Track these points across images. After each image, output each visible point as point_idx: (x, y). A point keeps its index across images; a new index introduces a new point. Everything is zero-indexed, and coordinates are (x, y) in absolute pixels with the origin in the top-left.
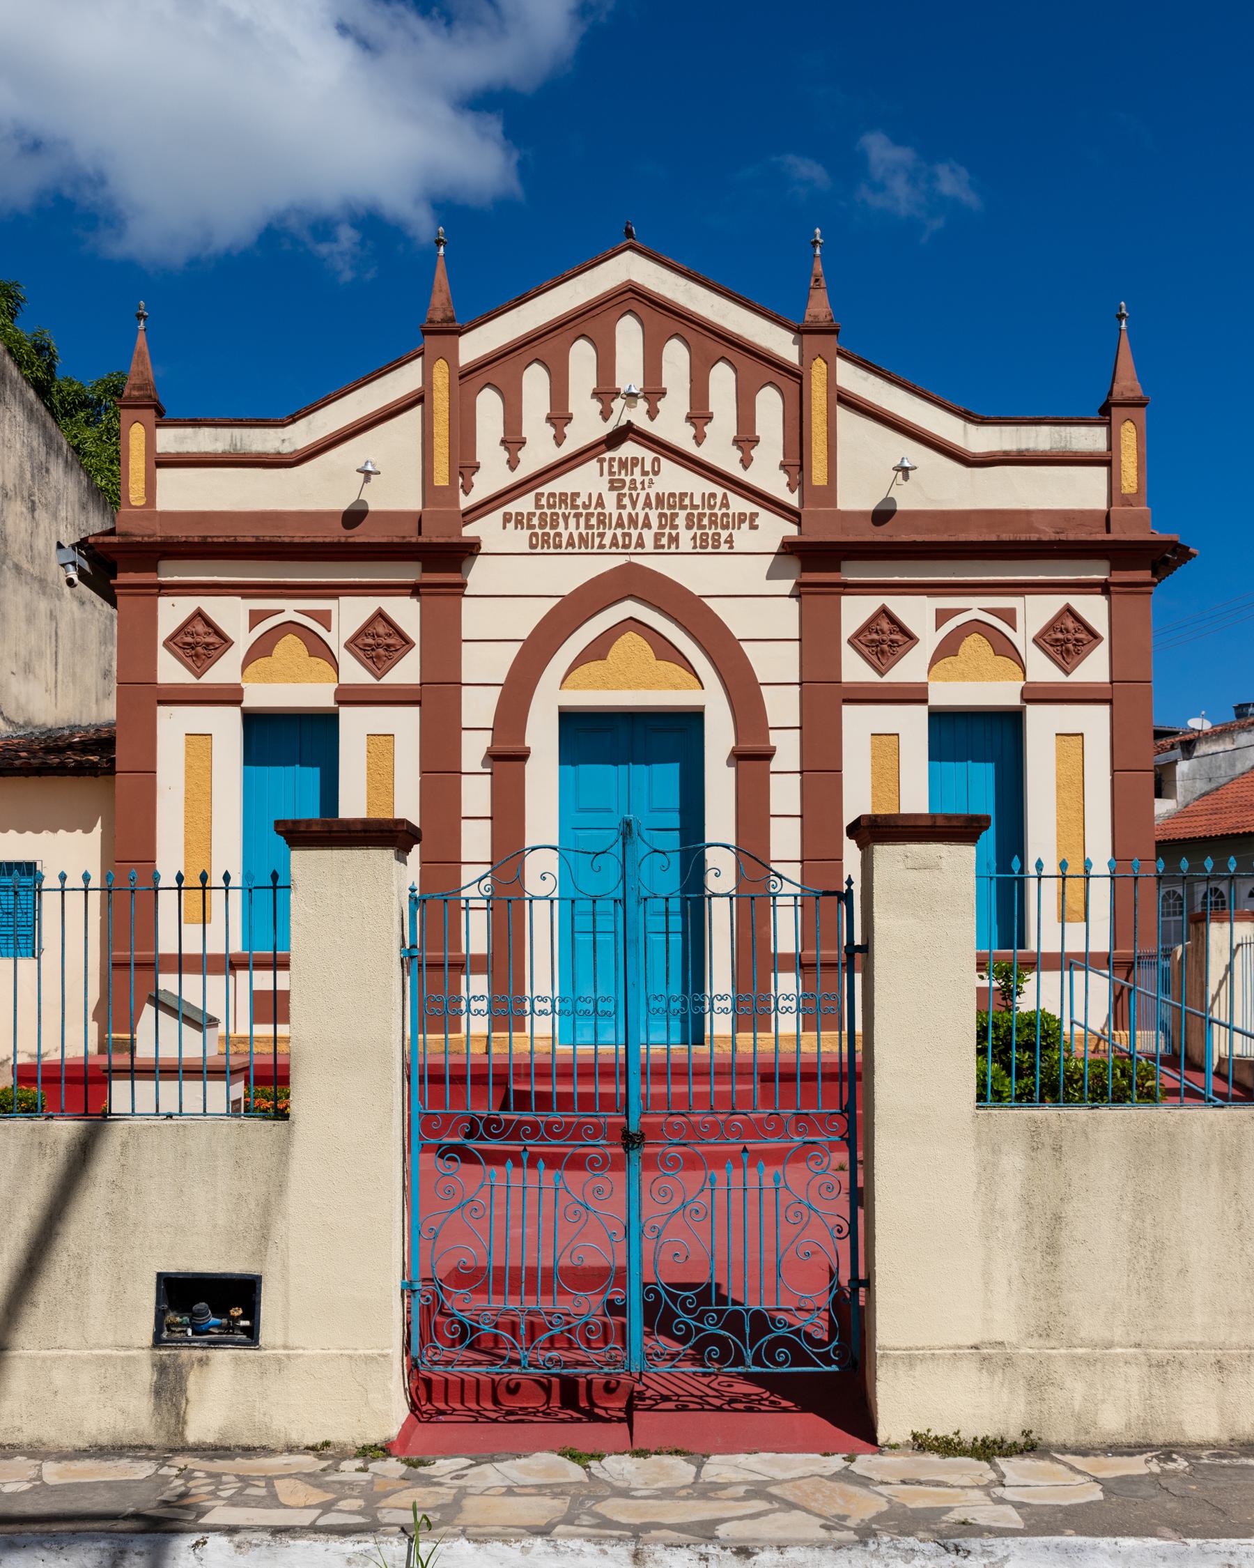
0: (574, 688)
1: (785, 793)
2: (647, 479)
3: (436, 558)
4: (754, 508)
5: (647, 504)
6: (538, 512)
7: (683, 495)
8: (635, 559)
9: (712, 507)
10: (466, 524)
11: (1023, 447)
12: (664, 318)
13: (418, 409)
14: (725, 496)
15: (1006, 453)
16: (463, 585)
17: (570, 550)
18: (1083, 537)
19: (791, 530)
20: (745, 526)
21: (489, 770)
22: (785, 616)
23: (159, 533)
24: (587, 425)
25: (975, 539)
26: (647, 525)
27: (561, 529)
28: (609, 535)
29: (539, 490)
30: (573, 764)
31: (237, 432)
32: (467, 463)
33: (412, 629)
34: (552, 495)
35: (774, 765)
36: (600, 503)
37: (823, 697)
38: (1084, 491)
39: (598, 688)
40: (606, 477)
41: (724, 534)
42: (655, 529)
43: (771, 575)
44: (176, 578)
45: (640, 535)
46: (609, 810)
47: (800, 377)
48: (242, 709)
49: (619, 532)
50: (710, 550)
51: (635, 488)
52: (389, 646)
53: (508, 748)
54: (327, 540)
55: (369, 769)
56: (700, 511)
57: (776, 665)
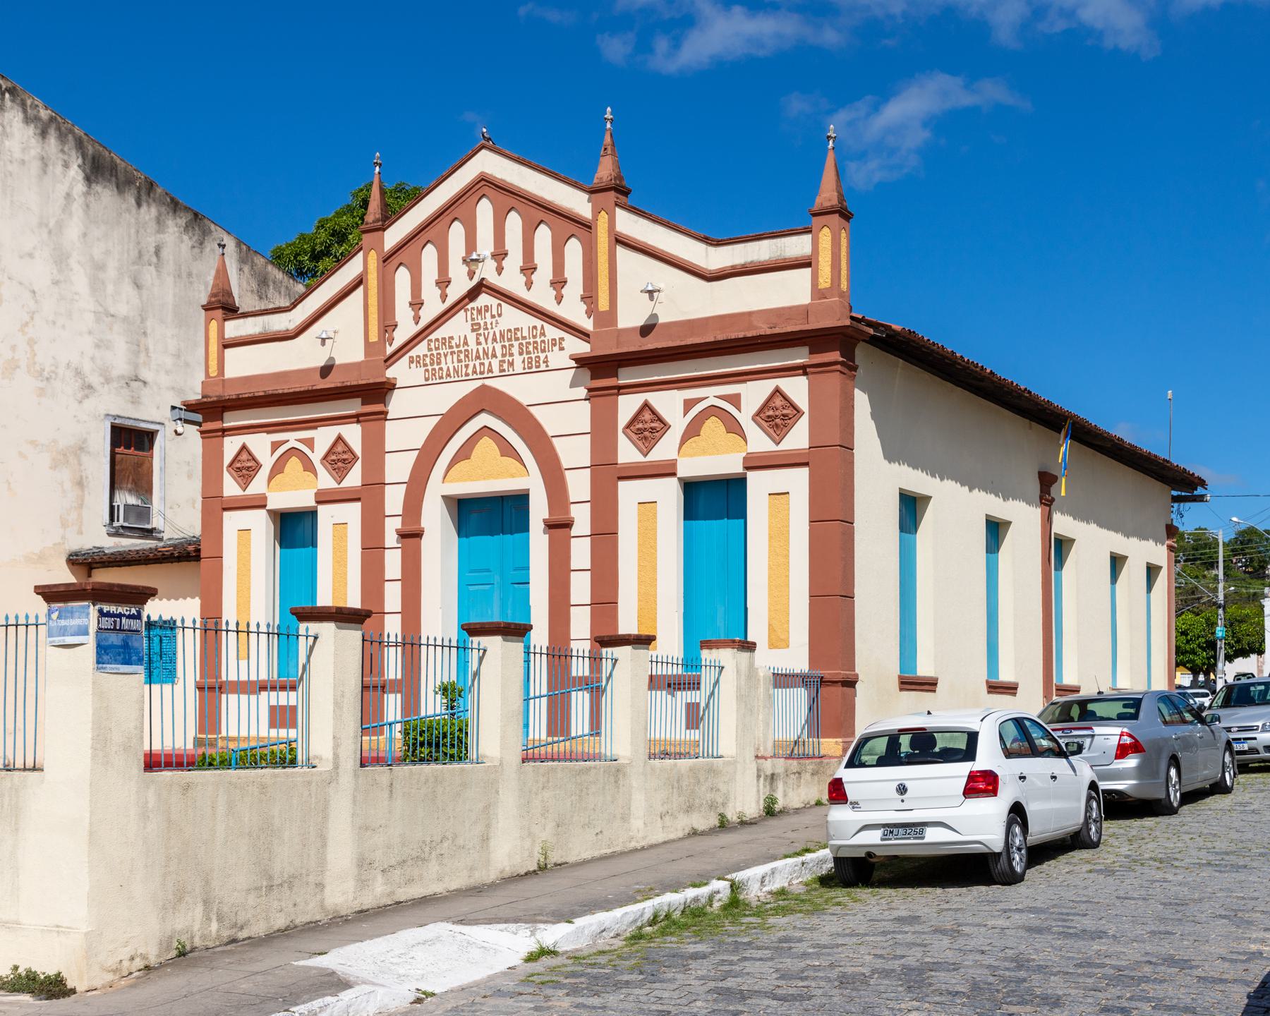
1: (581, 553)
5: (494, 340)
7: (517, 329)
8: (487, 382)
9: (534, 337)
10: (388, 367)
11: (749, 260)
13: (361, 288)
15: (733, 267)
16: (386, 413)
18: (789, 329)
19: (583, 348)
20: (556, 348)
22: (580, 415)
23: (231, 393)
24: (460, 285)
26: (494, 356)
27: (443, 365)
30: (467, 536)
31: (266, 318)
32: (388, 323)
33: (357, 448)
34: (437, 340)
36: (466, 343)
37: (608, 474)
40: (470, 322)
41: (542, 356)
42: (500, 358)
43: (573, 385)
44: (232, 424)
48: (272, 513)
49: (477, 363)
50: (534, 369)
53: (411, 528)
57: (575, 454)
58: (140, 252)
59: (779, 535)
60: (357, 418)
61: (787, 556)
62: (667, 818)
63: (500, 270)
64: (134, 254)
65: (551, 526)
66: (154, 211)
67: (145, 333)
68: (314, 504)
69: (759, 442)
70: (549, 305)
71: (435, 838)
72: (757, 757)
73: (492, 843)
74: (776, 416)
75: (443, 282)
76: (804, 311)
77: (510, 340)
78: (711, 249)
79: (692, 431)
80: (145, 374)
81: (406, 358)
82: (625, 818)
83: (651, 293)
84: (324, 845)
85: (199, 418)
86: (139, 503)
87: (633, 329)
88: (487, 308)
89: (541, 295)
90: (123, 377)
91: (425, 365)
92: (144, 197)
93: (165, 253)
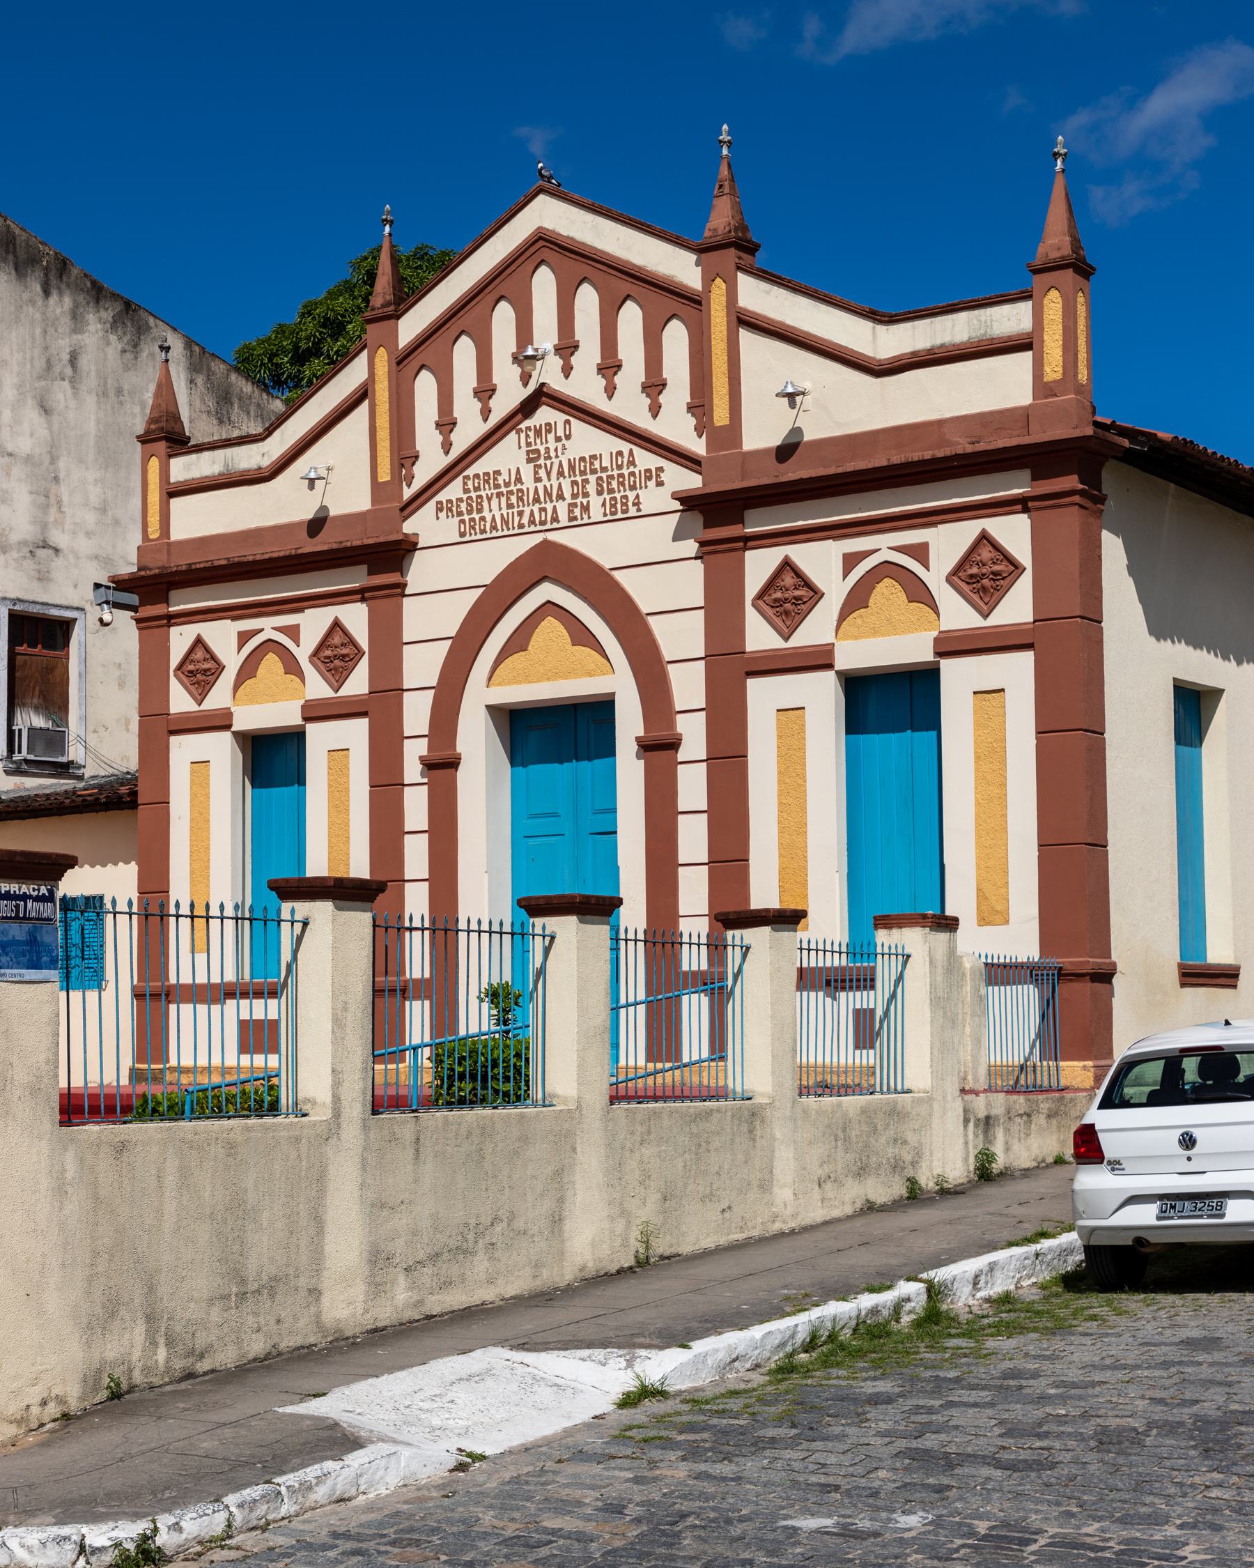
0: (499, 684)
1: (692, 786)
2: (559, 445)
3: (378, 559)
4: (661, 462)
5: (561, 474)
6: (465, 497)
7: (593, 457)
8: (551, 536)
9: (620, 467)
10: (406, 518)
11: (938, 342)
12: (577, 262)
13: (365, 405)
14: (631, 451)
15: (914, 354)
16: (405, 585)
17: (494, 534)
18: (1001, 444)
19: (692, 481)
20: (651, 484)
21: (425, 780)
22: (690, 582)
23: (180, 562)
25: (864, 467)
26: (561, 497)
27: (486, 513)
28: (527, 510)
29: (465, 474)
30: (524, 766)
31: (228, 452)
33: (363, 640)
34: (477, 476)
35: (681, 757)
36: (519, 480)
37: (730, 668)
38: (1000, 388)
39: (520, 682)
40: (524, 449)
41: (631, 495)
42: (569, 500)
43: (676, 538)
44: (182, 607)
45: (555, 507)
46: (556, 815)
47: (699, 303)
48: (241, 737)
49: (536, 508)
50: (620, 516)
51: (549, 458)
52: (344, 656)
53: (443, 754)
54: (281, 554)
55: (330, 786)
56: (610, 473)
57: (682, 639)
58: (48, 361)
59: (991, 754)
60: (361, 594)
61: (1003, 785)
62: (828, 1186)
63: (567, 370)
64: (40, 364)
65: (647, 747)
66: (67, 301)
67: (56, 479)
68: (299, 721)
69: (958, 614)
70: (639, 417)
71: (482, 1220)
72: (963, 1091)
73: (568, 1226)
74: (983, 575)
75: (485, 391)
76: (1021, 416)
77: (583, 473)
78: (881, 328)
79: (856, 600)
80: (58, 538)
81: (432, 505)
82: (765, 1186)
83: (791, 397)
84: (320, 1232)
85: (134, 599)
86: (50, 725)
87: (765, 452)
88: (549, 427)
89: (629, 405)
90: (24, 543)
91: (460, 514)
92: (54, 282)
93: (85, 362)
